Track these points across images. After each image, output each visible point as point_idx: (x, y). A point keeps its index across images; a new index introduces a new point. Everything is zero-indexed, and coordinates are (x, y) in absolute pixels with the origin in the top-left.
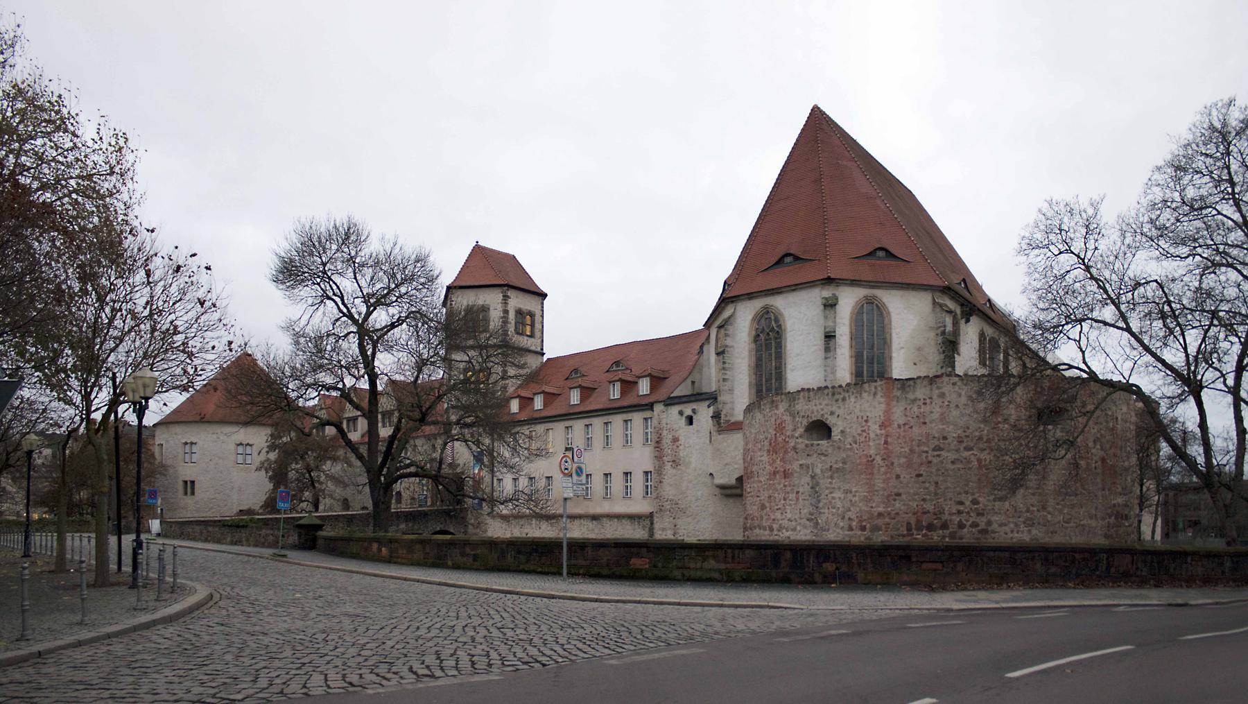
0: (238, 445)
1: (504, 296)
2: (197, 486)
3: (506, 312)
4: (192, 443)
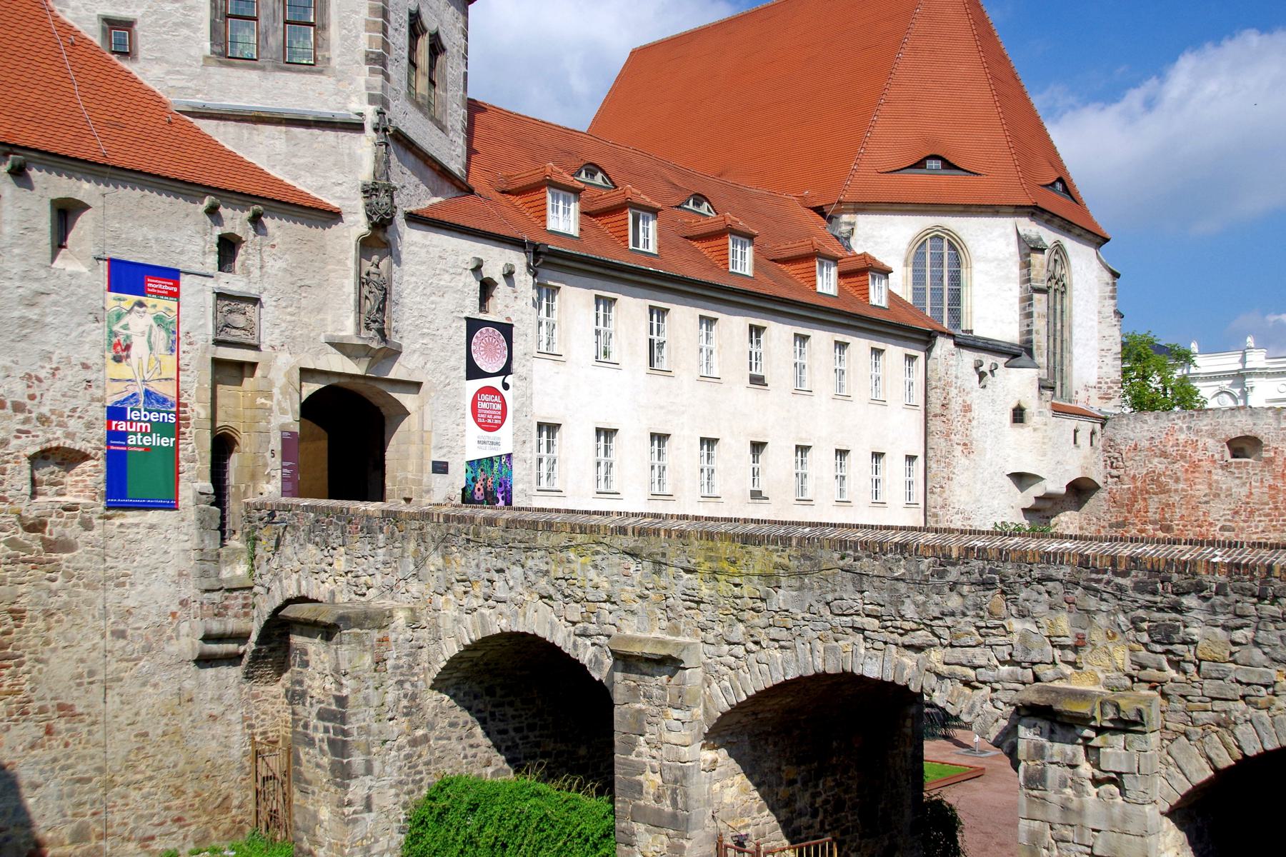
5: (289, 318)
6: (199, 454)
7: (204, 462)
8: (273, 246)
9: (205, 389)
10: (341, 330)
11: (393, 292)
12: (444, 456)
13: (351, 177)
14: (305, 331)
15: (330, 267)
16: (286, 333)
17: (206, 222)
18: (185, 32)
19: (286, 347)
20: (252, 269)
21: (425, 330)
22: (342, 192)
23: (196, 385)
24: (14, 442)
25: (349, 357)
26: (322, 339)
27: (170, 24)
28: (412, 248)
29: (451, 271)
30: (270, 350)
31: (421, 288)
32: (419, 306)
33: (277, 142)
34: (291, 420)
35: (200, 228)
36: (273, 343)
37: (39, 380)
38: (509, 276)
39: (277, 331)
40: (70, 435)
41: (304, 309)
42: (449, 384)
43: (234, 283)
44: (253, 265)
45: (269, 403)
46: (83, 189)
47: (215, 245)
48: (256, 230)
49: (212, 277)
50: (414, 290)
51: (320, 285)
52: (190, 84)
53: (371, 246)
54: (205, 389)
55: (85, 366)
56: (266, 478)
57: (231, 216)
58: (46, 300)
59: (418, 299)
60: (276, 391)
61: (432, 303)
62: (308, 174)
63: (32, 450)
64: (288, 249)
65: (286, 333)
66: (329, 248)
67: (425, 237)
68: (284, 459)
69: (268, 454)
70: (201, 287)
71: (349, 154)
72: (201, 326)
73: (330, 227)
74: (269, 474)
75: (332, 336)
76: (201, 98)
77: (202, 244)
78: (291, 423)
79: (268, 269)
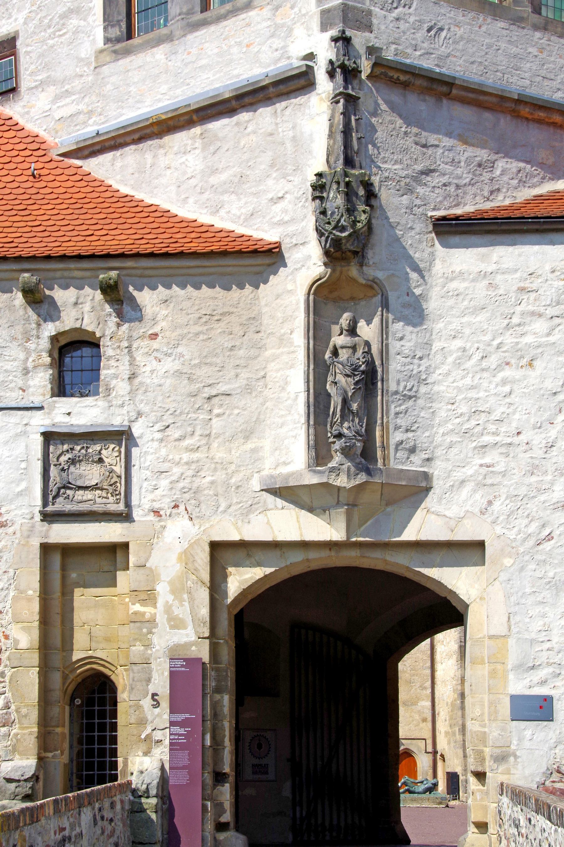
5: (186, 457)
6: (17, 711)
7: (26, 722)
8: (154, 336)
9: (29, 599)
10: (285, 464)
11: (393, 377)
12: (543, 683)
13: (297, 180)
14: (220, 476)
15: (268, 353)
16: (181, 485)
17: (27, 320)
18: (74, 22)
19: (182, 508)
20: (114, 382)
21: (487, 439)
22: (285, 211)
23: (12, 594)
25: (311, 510)
27: (56, 19)
28: (453, 285)
29: (550, 312)
30: (151, 517)
31: (477, 357)
32: (473, 394)
33: (190, 157)
34: (193, 638)
35: (18, 330)
36: (156, 506)
39: (164, 483)
41: (218, 436)
42: (549, 537)
44: (116, 376)
45: (148, 610)
47: (45, 355)
48: (120, 314)
49: (41, 408)
50: (458, 364)
51: (248, 389)
52: (81, 107)
53: (352, 298)
54: (29, 599)
56: (144, 747)
57: (73, 300)
59: (468, 381)
61: (504, 382)
62: (233, 197)
64: (183, 337)
65: (181, 485)
66: (266, 320)
67: (483, 258)
68: (173, 710)
69: (147, 702)
70: (20, 429)
71: (294, 139)
72: (20, 494)
73: (266, 282)
74: (148, 737)
75: (272, 477)
76: (95, 123)
77: (22, 356)
78: (191, 644)
79: (144, 378)
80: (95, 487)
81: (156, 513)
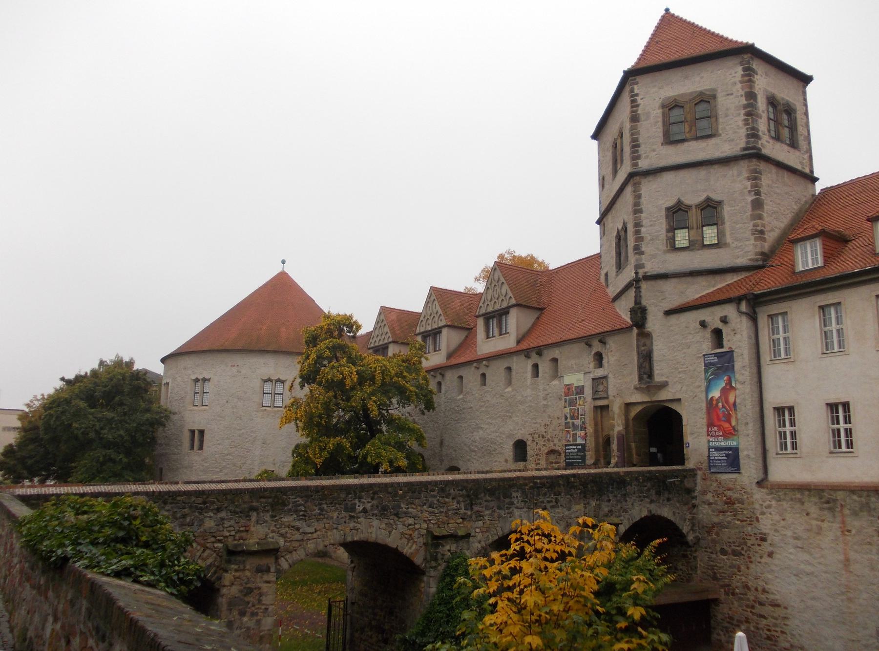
0: (265, 381)
1: (744, 70)
2: (207, 436)
3: (751, 96)
4: (205, 380)
5: (619, 381)
21: (680, 370)
24: (542, 449)
26: (633, 388)
30: (613, 398)
37: (548, 425)
38: (724, 320)
40: (555, 445)
43: (599, 373)
46: (556, 353)
55: (558, 418)
58: (548, 396)
60: (616, 416)
63: (546, 451)
80: (602, 391)
81: (614, 396)
